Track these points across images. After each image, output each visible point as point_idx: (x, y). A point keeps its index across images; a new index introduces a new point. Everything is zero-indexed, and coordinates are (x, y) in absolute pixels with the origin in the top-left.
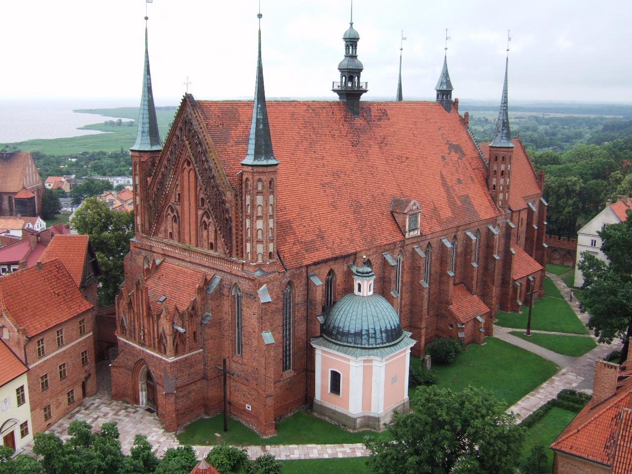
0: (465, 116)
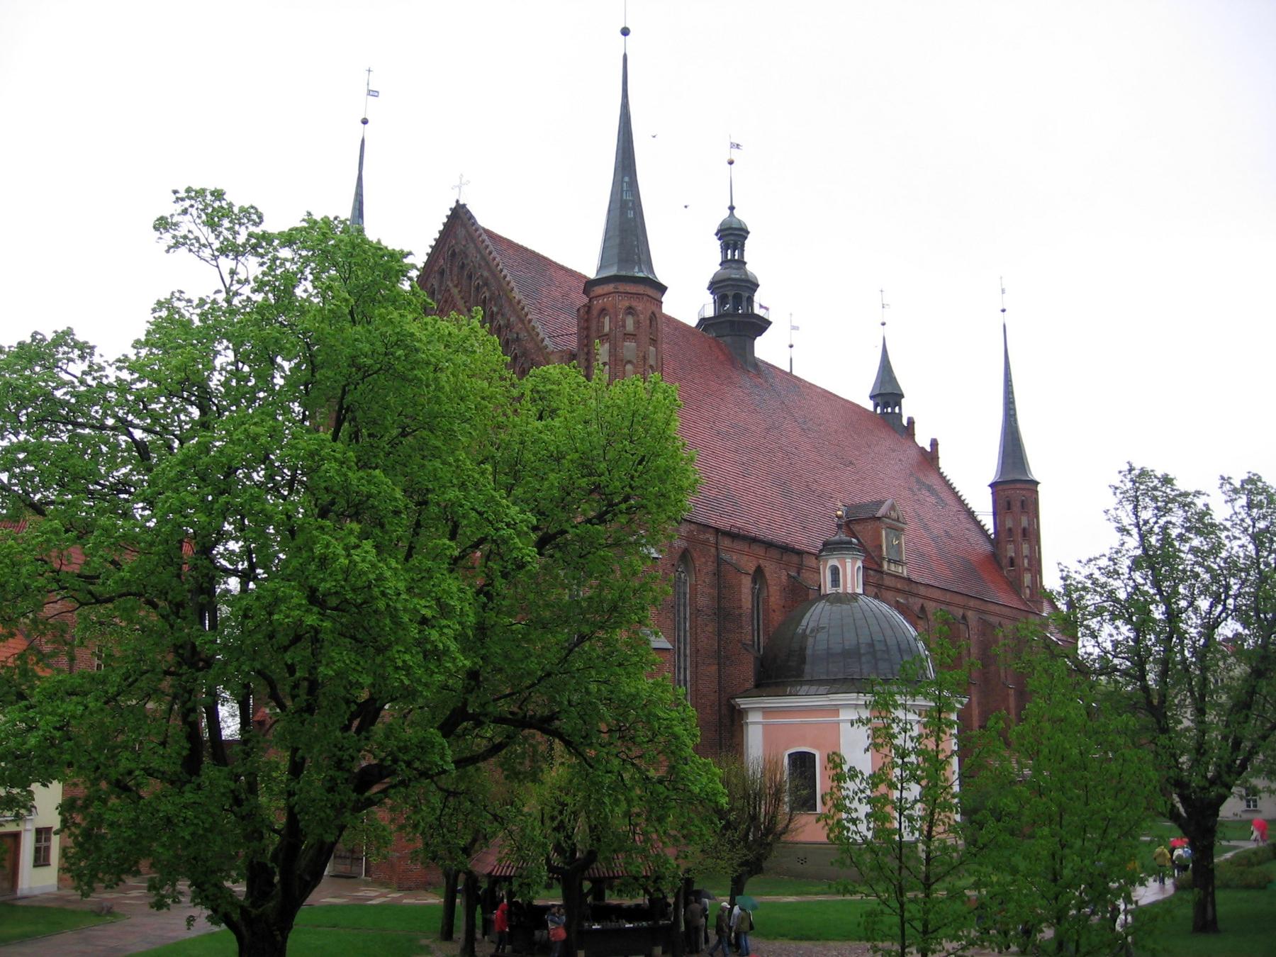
0: (931, 445)
